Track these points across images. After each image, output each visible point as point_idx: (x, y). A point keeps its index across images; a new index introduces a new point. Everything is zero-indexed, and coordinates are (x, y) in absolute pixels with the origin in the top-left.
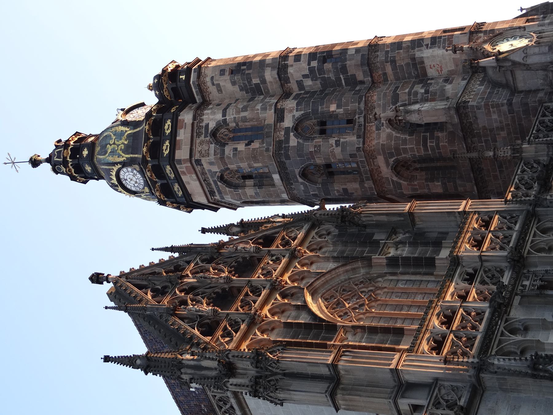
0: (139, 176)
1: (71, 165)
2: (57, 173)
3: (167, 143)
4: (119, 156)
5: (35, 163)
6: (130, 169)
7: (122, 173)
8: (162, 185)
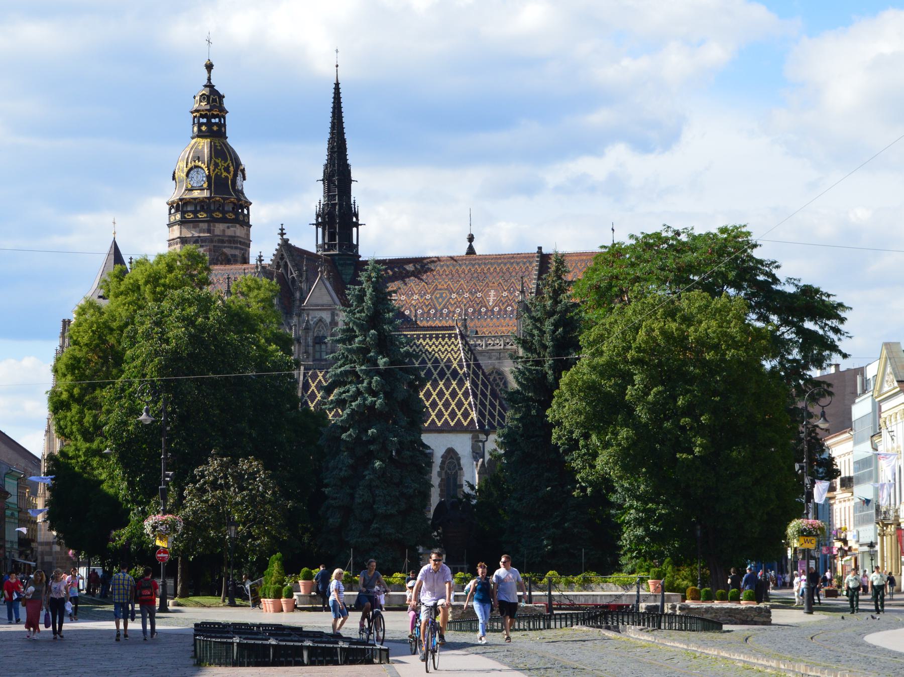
3: (221, 215)
4: (214, 171)
5: (209, 67)
6: (204, 179)
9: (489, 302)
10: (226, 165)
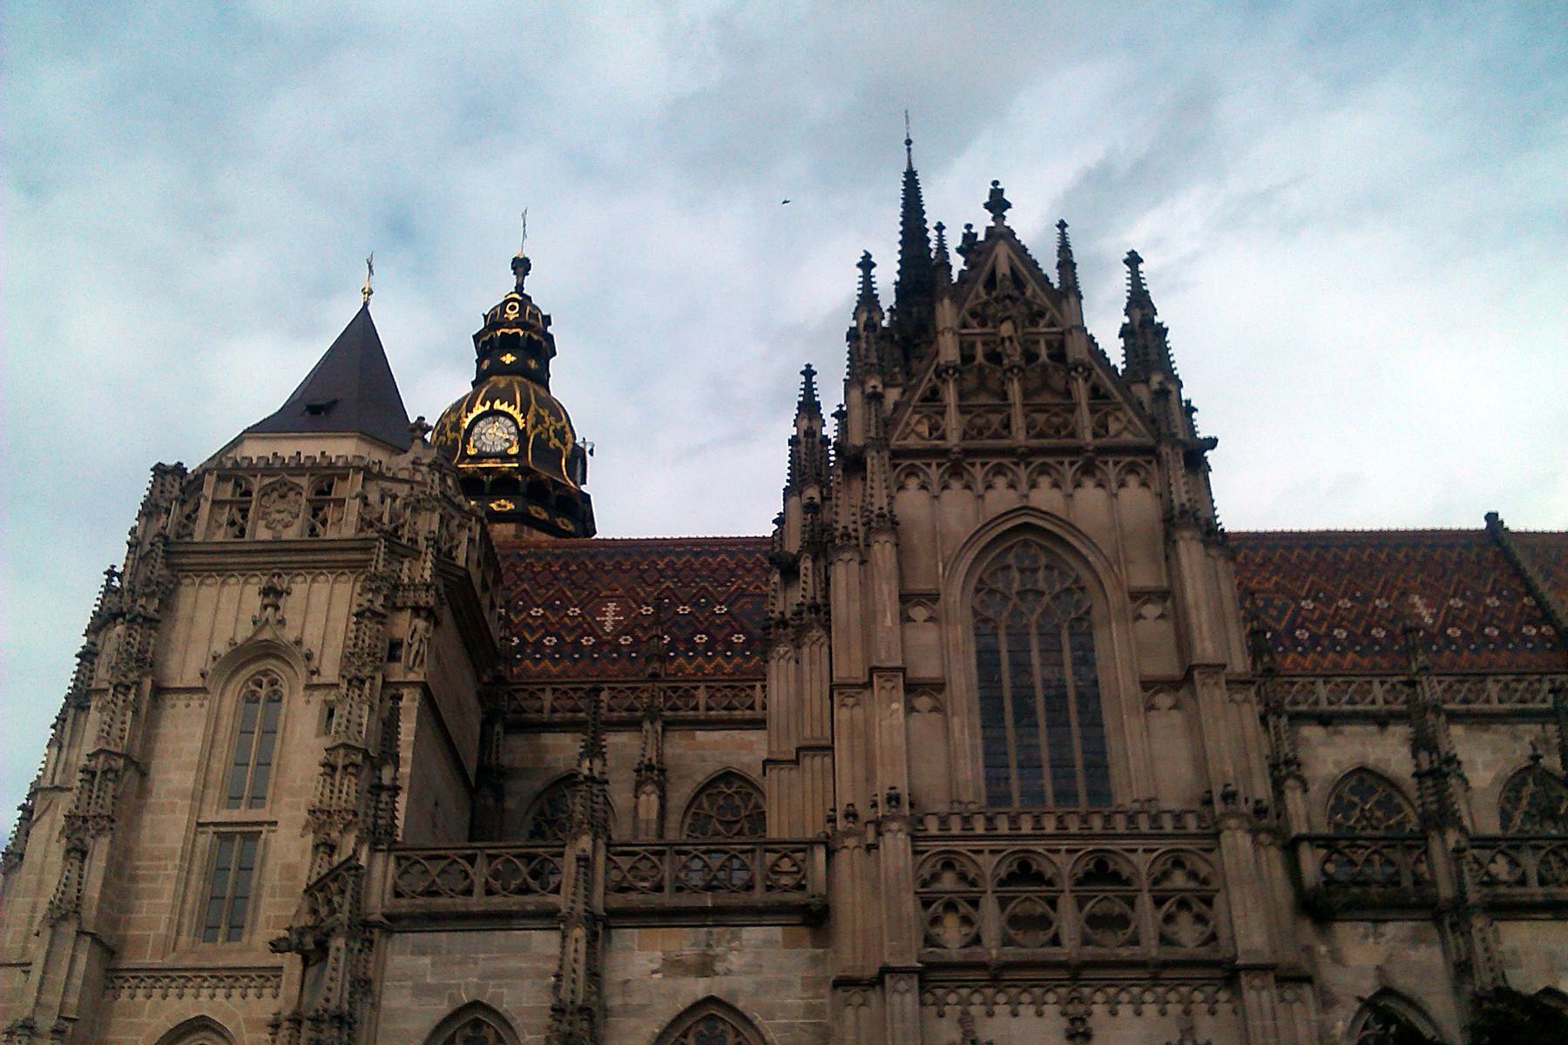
0: (498, 449)
3: (545, 516)
4: (534, 427)
5: (521, 266)
7: (509, 423)
9: (1419, 617)
10: (559, 426)
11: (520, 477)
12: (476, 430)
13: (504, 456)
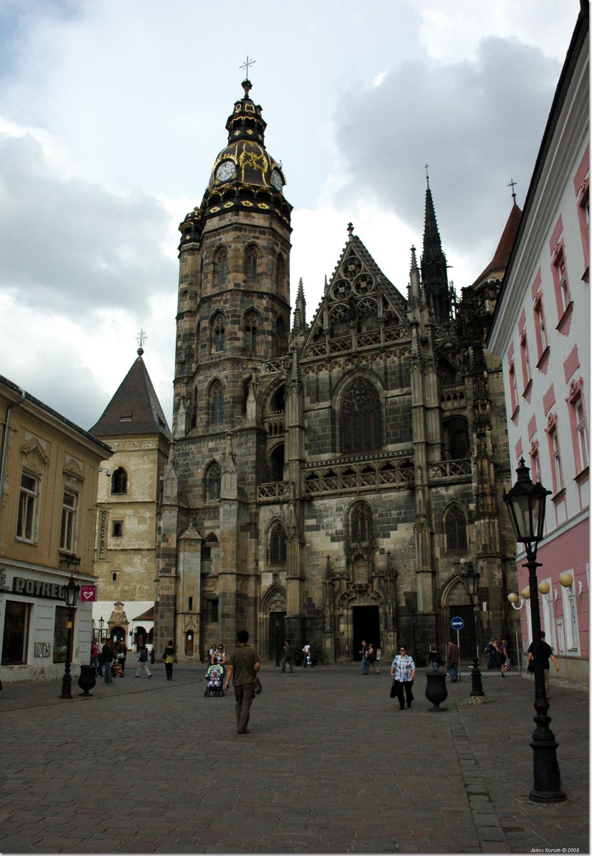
0: (228, 178)
1: (241, 119)
2: (236, 104)
3: (251, 204)
4: (243, 162)
5: (247, 85)
6: (233, 170)
7: (231, 163)
8: (220, 196)
11: (235, 189)
12: (218, 172)
13: (230, 181)
